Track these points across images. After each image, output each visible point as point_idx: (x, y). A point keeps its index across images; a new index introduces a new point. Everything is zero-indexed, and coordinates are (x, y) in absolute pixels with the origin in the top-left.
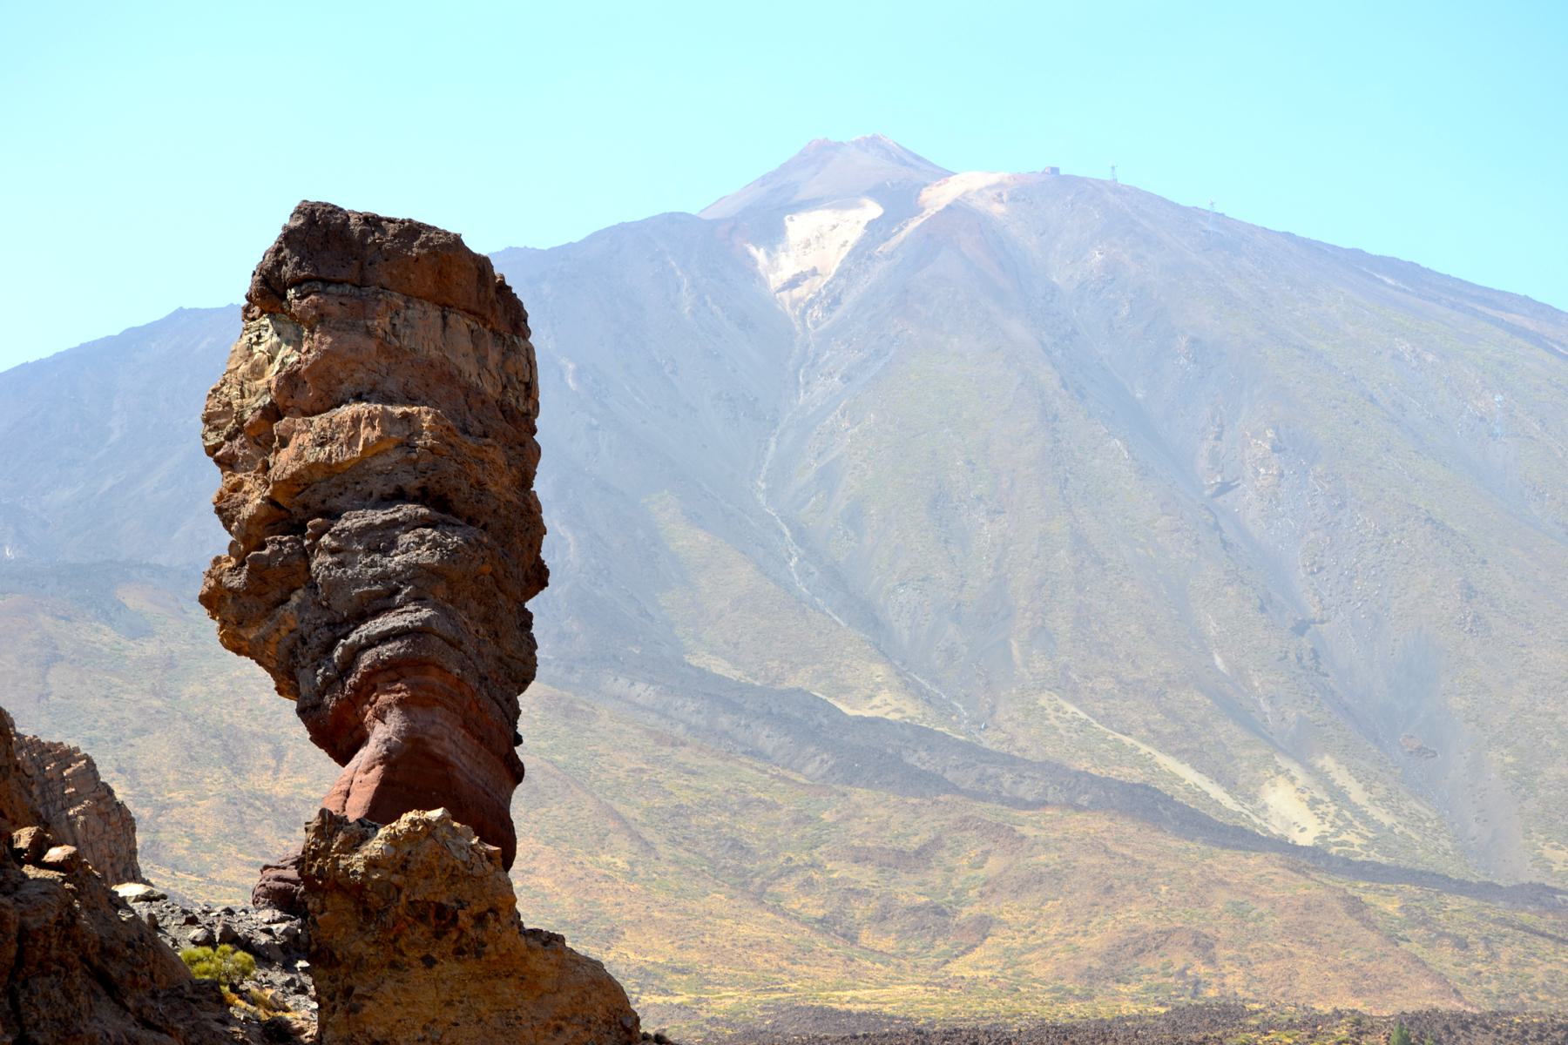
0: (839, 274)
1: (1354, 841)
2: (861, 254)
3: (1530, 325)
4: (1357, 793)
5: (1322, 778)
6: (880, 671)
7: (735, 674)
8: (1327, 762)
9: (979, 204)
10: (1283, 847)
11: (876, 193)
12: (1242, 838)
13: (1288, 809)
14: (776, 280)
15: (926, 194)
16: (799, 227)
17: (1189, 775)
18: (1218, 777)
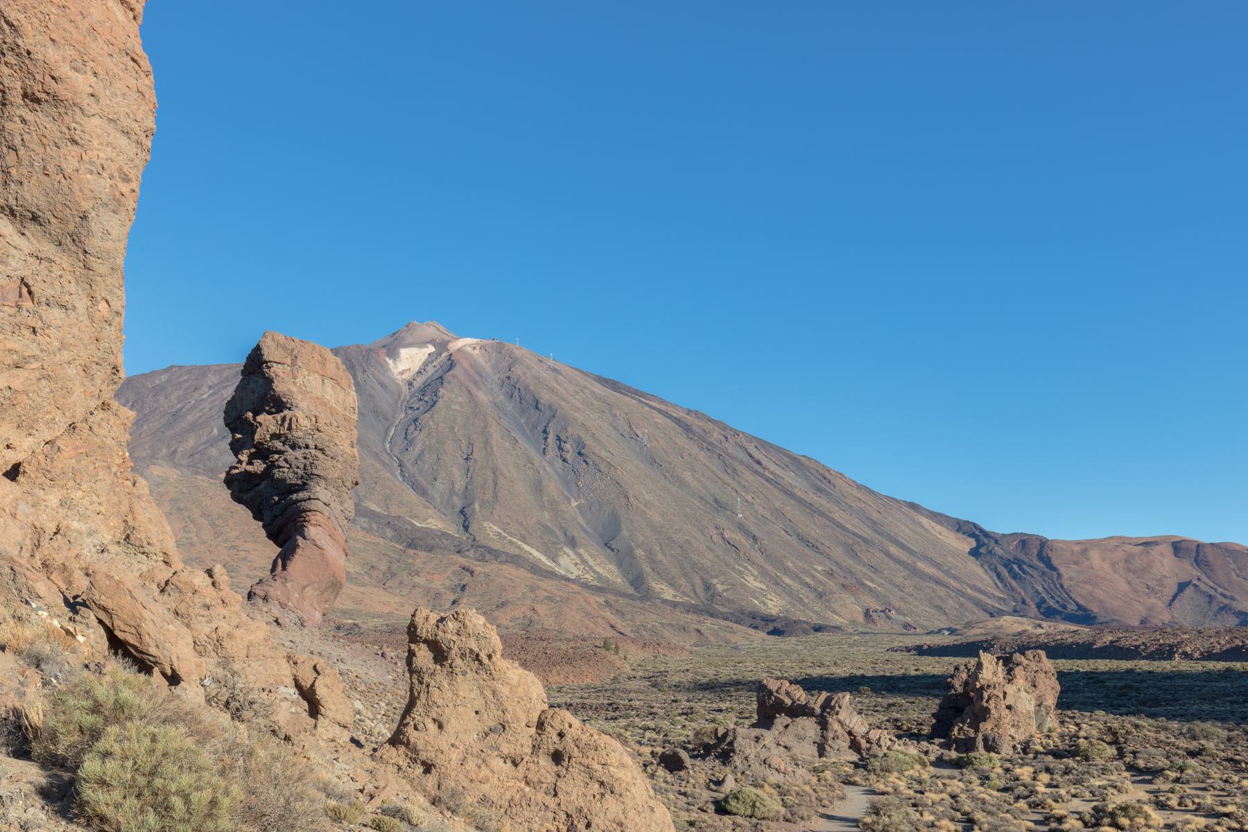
0: (419, 372)
1: (589, 577)
2: (426, 364)
3: (658, 406)
4: (591, 562)
5: (580, 556)
6: (430, 512)
7: (378, 510)
8: (582, 551)
9: (469, 349)
10: (568, 580)
11: (432, 342)
12: (550, 575)
13: (567, 563)
14: (395, 372)
15: (450, 345)
16: (404, 352)
17: (535, 553)
18: (544, 553)
